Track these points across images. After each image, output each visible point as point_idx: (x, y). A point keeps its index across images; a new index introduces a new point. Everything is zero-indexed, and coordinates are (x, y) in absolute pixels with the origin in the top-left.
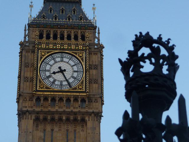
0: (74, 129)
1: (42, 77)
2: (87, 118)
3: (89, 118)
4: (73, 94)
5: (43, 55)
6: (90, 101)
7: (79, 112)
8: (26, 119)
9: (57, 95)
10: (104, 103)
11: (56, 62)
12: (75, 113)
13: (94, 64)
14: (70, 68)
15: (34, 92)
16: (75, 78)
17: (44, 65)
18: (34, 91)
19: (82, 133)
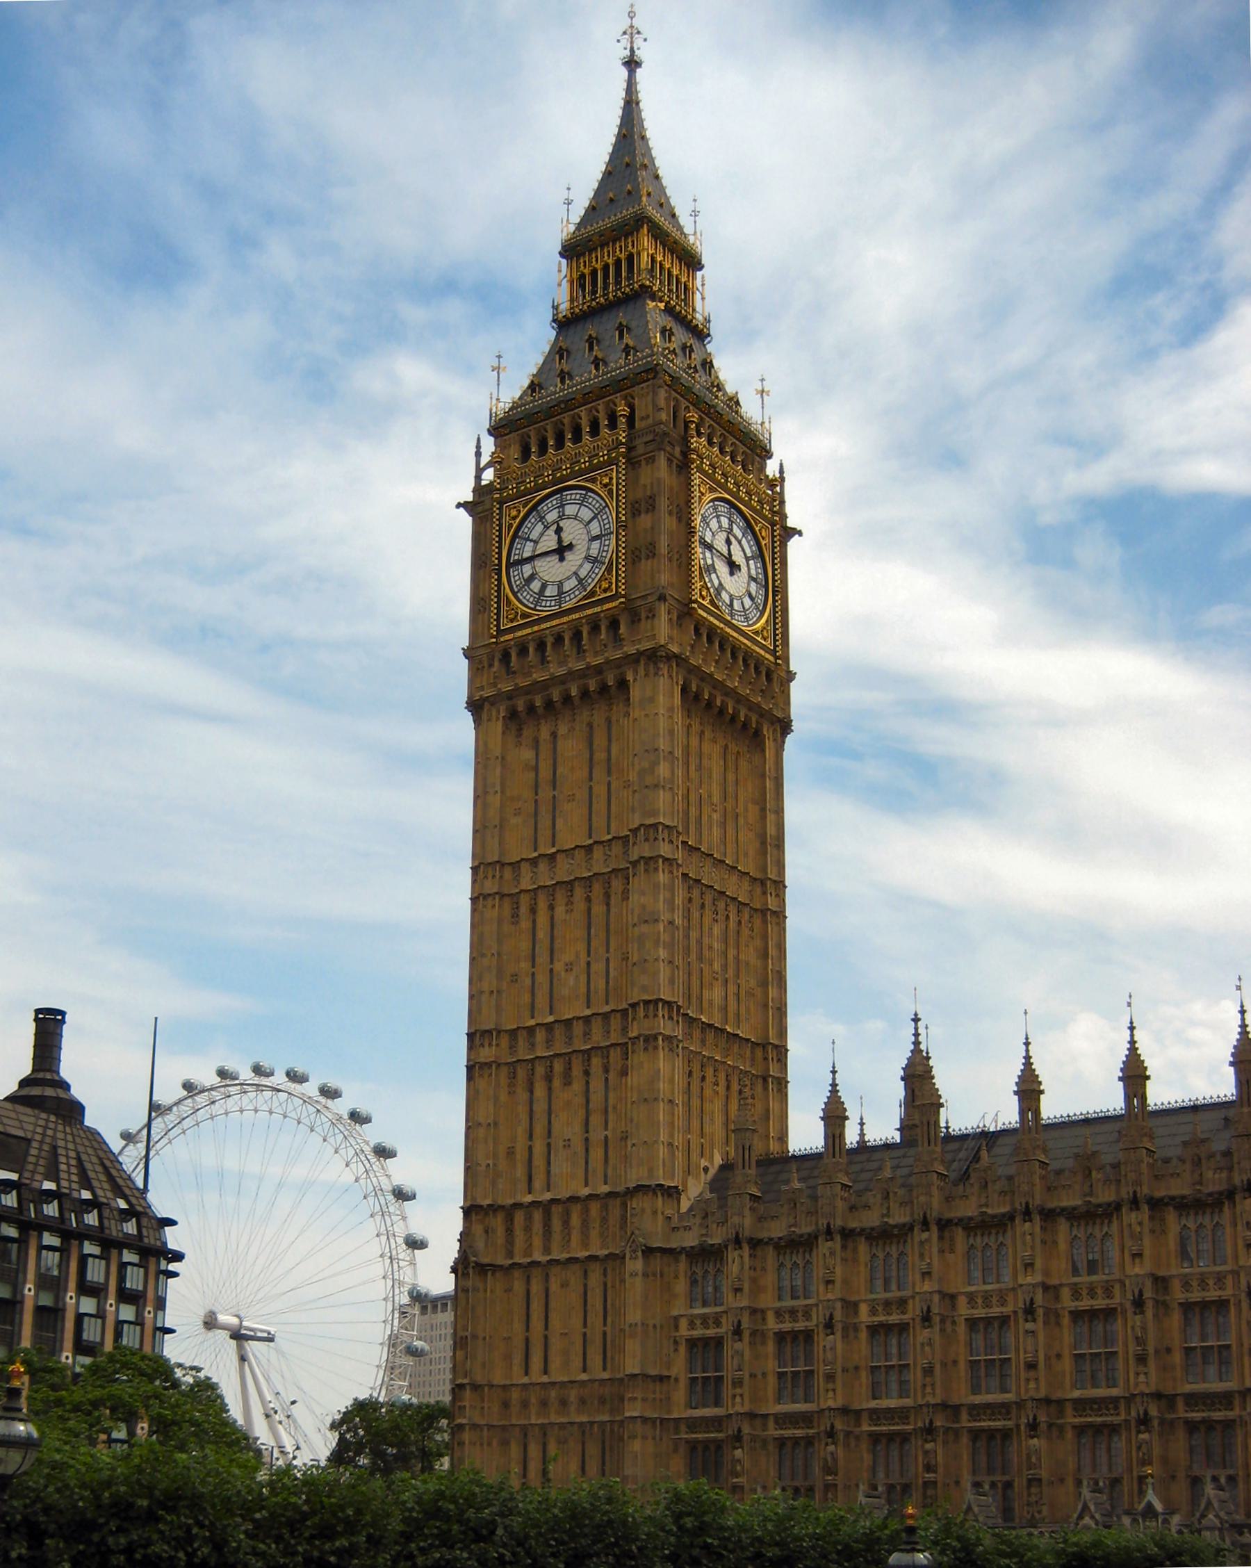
3: (636, 672)
5: (514, 518)
7: (608, 662)
11: (546, 528)
12: (599, 670)
13: (649, 493)
16: (594, 561)
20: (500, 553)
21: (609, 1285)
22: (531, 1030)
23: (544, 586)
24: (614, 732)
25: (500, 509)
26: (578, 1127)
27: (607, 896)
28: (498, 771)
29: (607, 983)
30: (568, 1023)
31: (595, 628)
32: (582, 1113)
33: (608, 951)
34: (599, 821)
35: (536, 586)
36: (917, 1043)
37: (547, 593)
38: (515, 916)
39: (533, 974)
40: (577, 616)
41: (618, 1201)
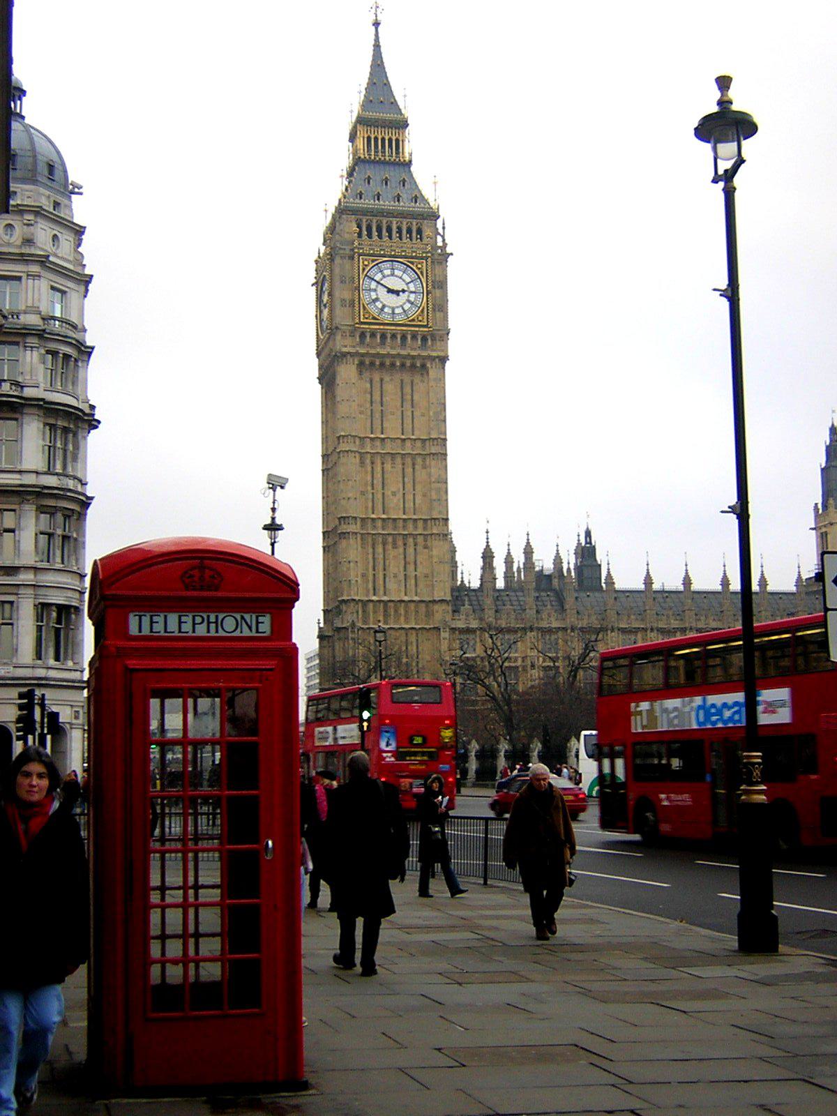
2: (429, 365)
3: (432, 364)
7: (419, 355)
12: (413, 357)
16: (412, 303)
21: (420, 641)
22: (373, 519)
23: (384, 306)
26: (402, 569)
27: (414, 464)
29: (414, 504)
30: (395, 520)
32: (403, 562)
34: (408, 427)
35: (379, 305)
36: (488, 542)
41: (423, 605)
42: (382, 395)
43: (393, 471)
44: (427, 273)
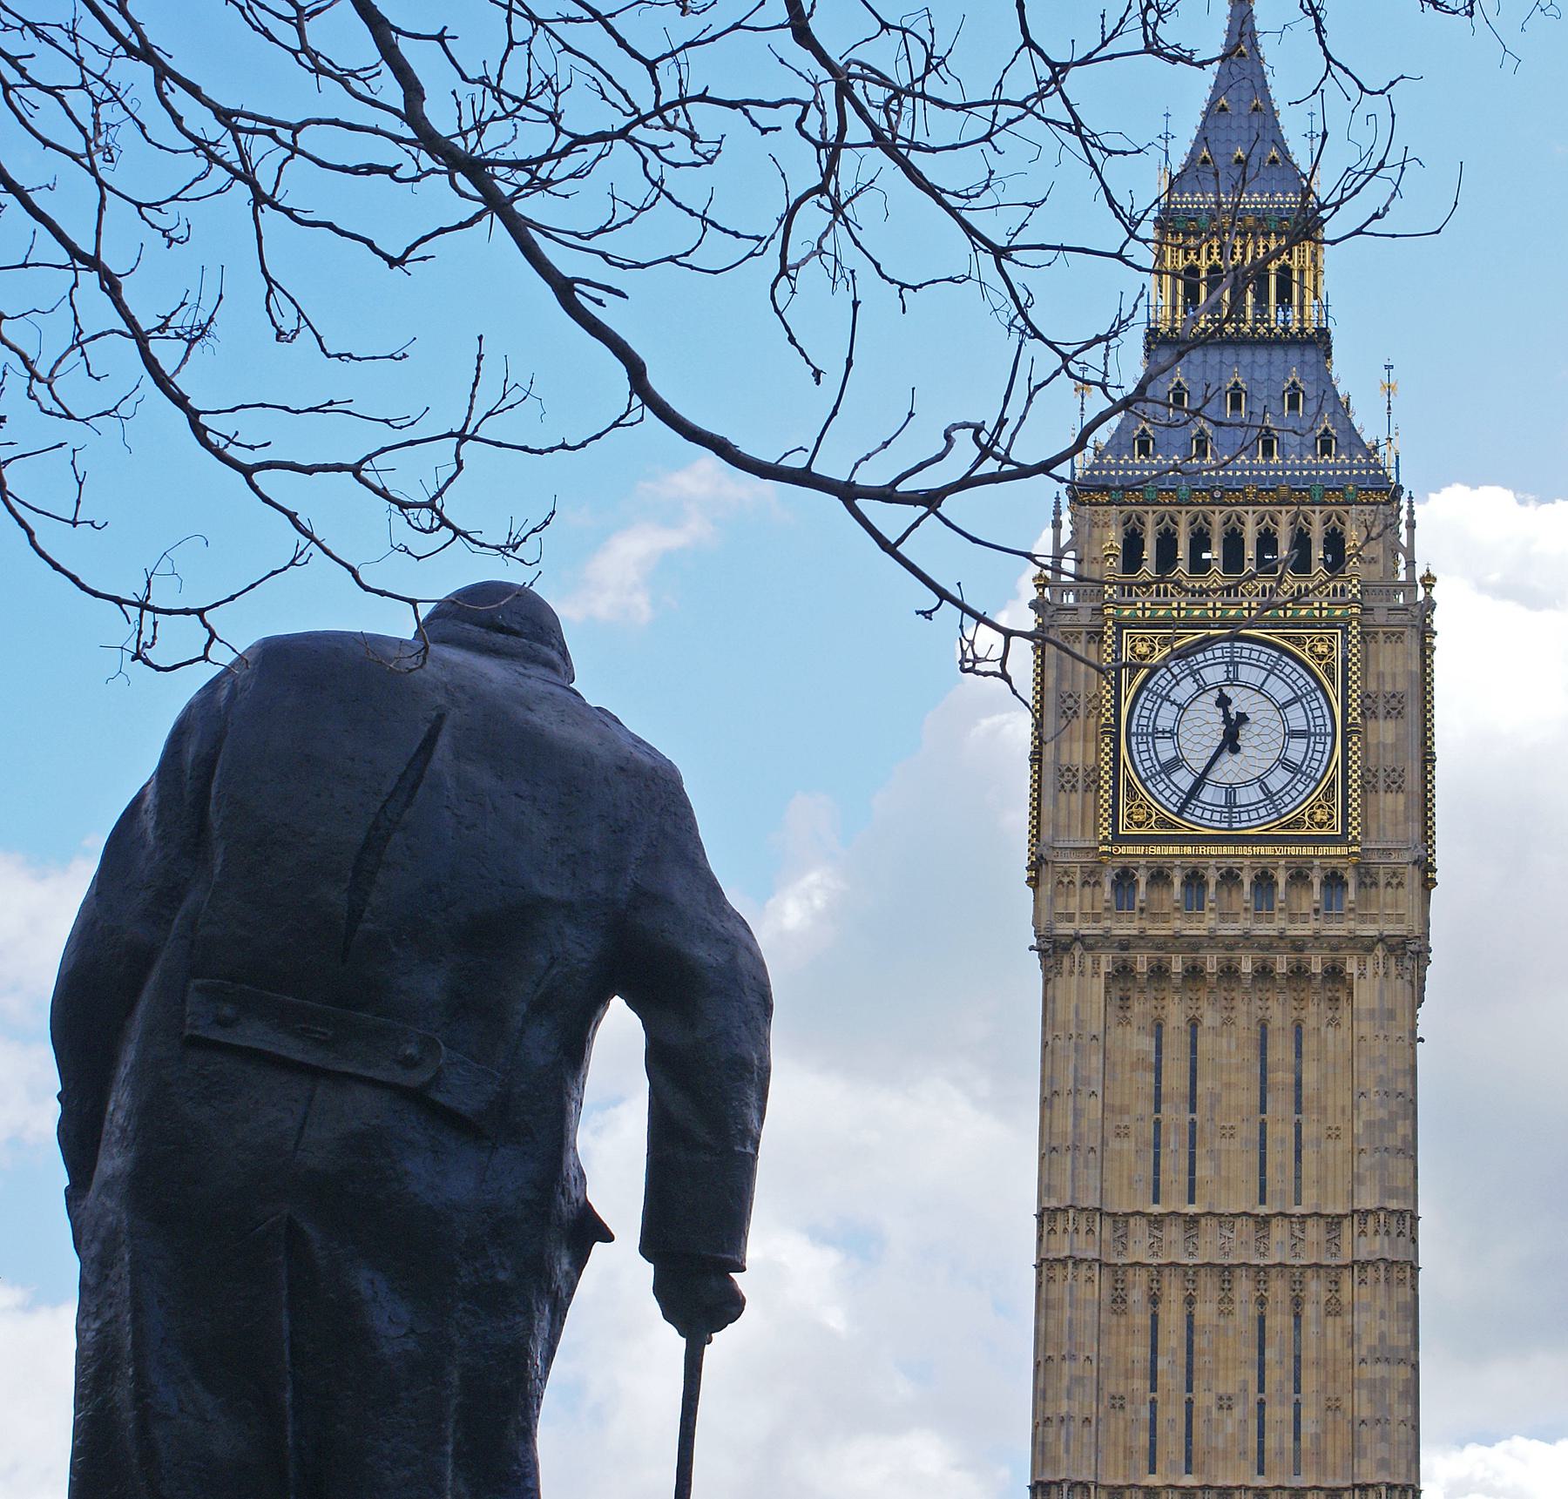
0: (1295, 1014)
1: (1140, 769)
2: (1352, 967)
3: (1362, 964)
4: (1283, 850)
6: (1368, 881)
8: (1071, 972)
9: (1212, 856)
10: (1437, 876)
11: (1203, 689)
12: (1298, 945)
13: (1388, 688)
14: (1270, 715)
15: (1105, 848)
16: (1295, 769)
17: (1149, 705)
18: (1105, 842)
19: (1330, 1036)
20: (1117, 707)
24: (1309, 1045)
25: (1119, 634)
27: (1297, 1302)
28: (1096, 1061)
29: (1297, 1437)
31: (1299, 877)
33: (1297, 1390)
37: (1207, 794)
38: (1119, 1301)
39: (1153, 1402)
40: (1269, 851)
42: (1193, 1070)
43: (1226, 1327)
44: (1345, 670)
